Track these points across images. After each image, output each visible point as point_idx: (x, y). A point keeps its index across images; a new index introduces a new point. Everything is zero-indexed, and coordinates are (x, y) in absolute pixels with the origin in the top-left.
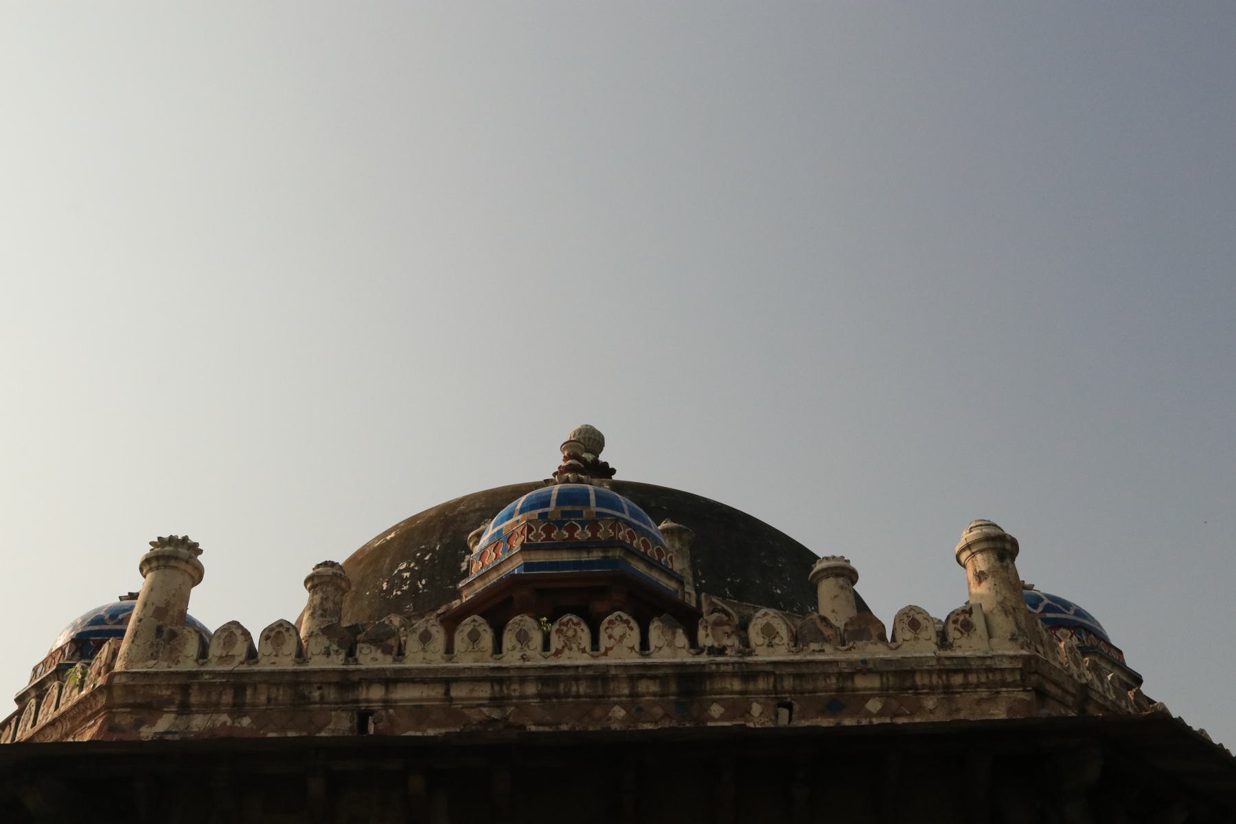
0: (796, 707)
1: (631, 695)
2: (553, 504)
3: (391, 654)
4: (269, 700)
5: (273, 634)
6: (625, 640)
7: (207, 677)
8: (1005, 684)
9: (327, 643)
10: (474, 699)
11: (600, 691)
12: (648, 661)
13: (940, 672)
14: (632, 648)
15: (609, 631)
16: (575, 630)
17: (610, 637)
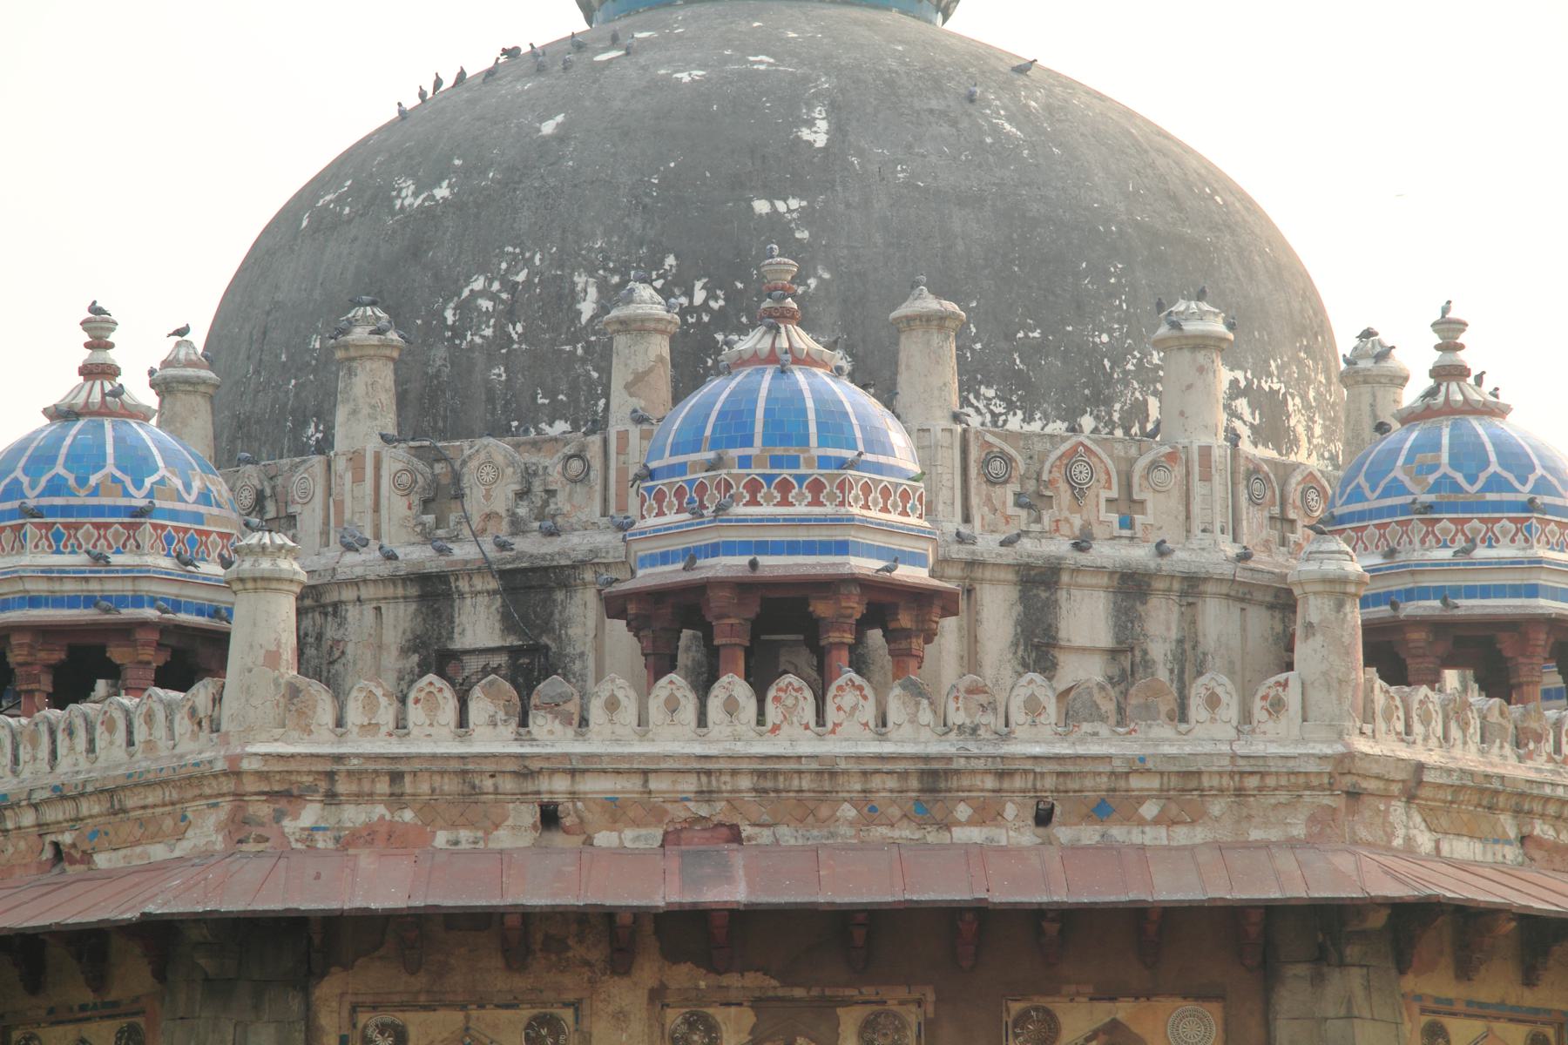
0: (1058, 810)
1: (864, 791)
2: (758, 440)
3: (571, 724)
4: (433, 791)
5: (422, 695)
6: (857, 713)
7: (355, 761)
8: (1309, 787)
9: (491, 709)
10: (678, 792)
11: (827, 786)
12: (887, 748)
13: (1232, 774)
14: (866, 725)
15: (838, 700)
16: (796, 698)
17: (839, 708)
